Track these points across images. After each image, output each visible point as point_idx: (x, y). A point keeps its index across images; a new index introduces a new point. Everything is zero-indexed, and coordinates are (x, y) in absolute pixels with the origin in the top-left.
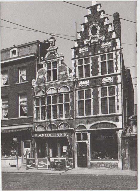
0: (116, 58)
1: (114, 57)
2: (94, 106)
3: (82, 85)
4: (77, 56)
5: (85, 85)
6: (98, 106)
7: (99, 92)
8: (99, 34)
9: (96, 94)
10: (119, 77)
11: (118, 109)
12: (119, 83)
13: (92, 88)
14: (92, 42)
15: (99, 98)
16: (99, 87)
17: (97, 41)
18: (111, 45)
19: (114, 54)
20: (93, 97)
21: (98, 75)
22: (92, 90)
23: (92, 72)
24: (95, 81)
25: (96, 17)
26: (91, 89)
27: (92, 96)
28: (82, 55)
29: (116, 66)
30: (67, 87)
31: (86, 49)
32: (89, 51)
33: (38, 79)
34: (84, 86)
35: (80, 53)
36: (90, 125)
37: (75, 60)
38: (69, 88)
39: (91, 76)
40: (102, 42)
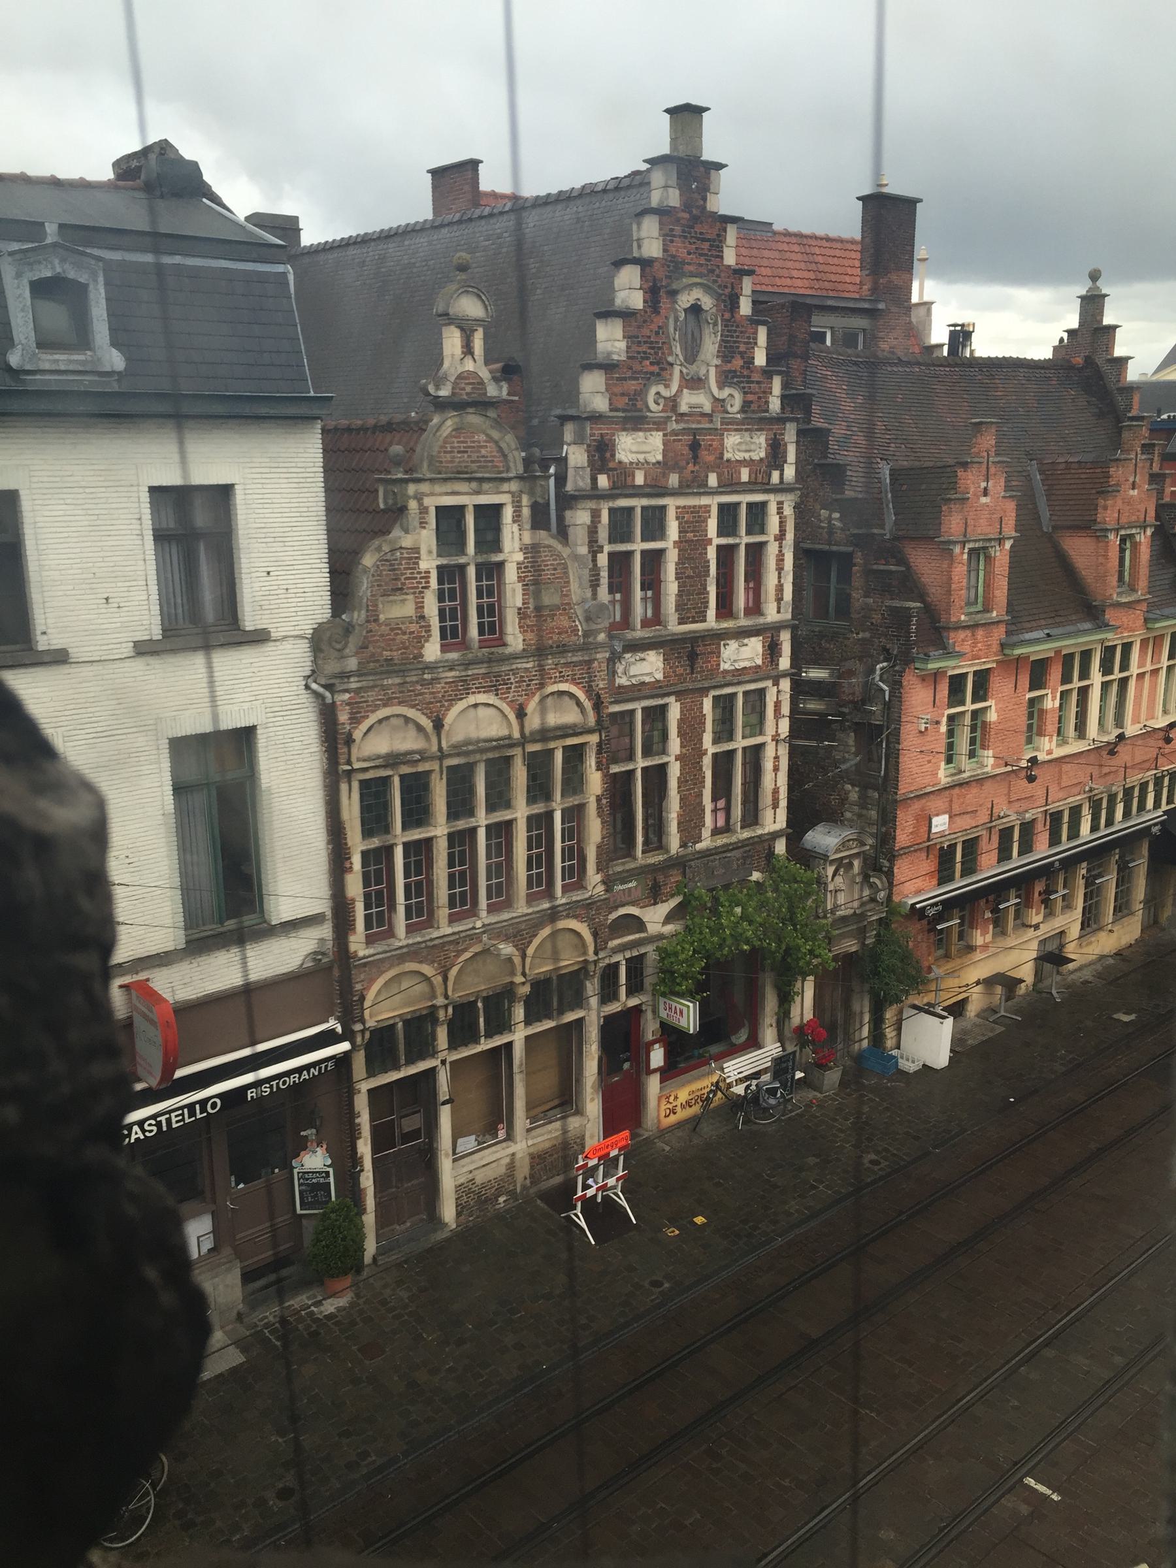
0: (780, 537)
1: (773, 522)
2: (681, 799)
3: (634, 676)
4: (603, 481)
5: (647, 679)
6: (700, 795)
7: (707, 717)
8: (716, 366)
9: (691, 730)
10: (785, 637)
11: (775, 806)
12: (784, 675)
13: (679, 695)
14: (684, 408)
15: (705, 753)
16: (704, 691)
17: (707, 408)
18: (763, 455)
19: (772, 508)
20: (682, 746)
21: (705, 621)
22: (675, 712)
23: (680, 595)
24: (693, 657)
25: (706, 245)
26: (672, 699)
27: (675, 745)
28: (629, 479)
29: (779, 577)
30: (571, 696)
31: (656, 441)
32: (666, 465)
33: (373, 626)
34: (643, 683)
35: (620, 462)
36: (664, 909)
37: (592, 504)
38: (588, 705)
39: (674, 627)
40: (731, 424)
